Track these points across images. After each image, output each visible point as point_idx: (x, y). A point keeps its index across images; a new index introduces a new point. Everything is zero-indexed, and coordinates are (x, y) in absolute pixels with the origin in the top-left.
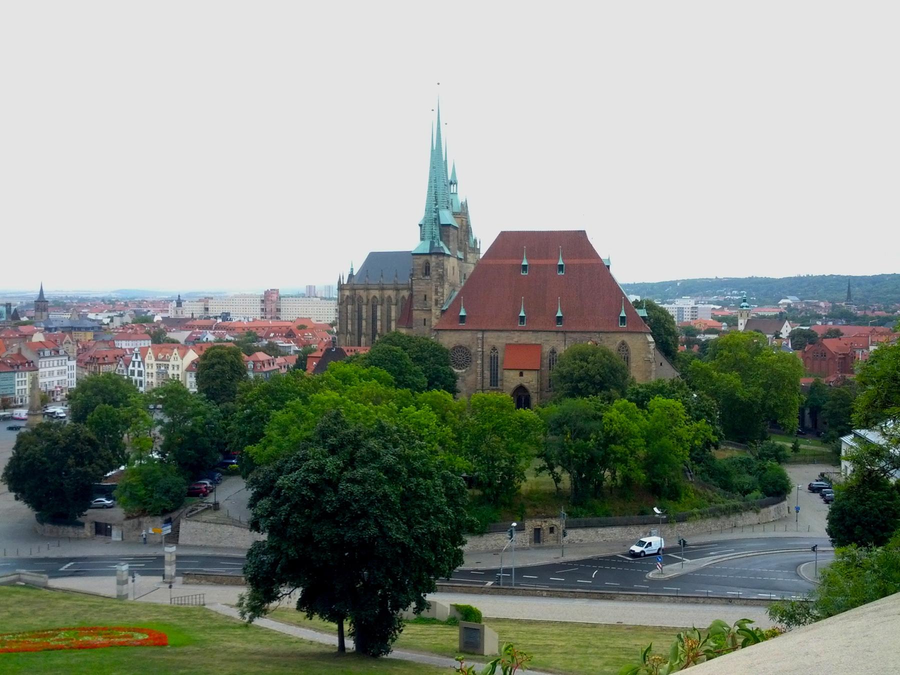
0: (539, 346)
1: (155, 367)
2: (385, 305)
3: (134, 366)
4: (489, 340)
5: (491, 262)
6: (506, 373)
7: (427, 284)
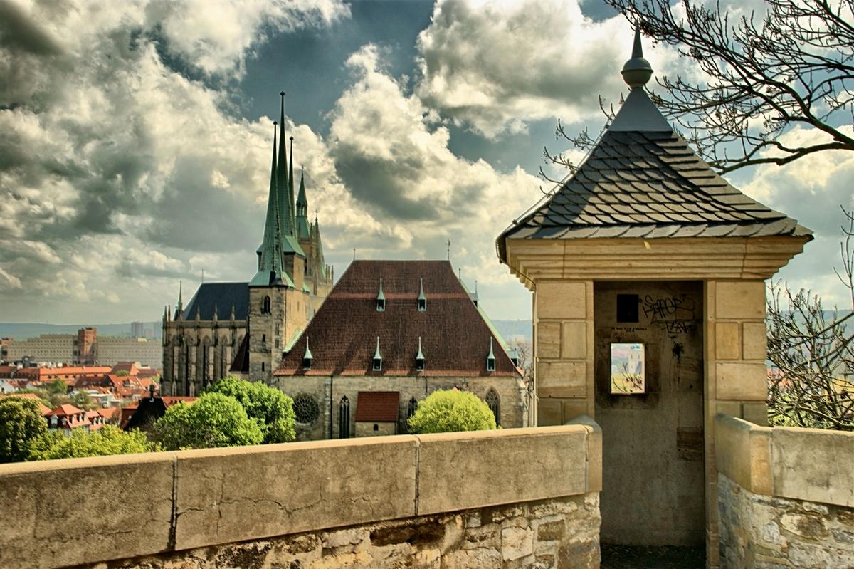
0: (396, 395)
2: (219, 347)
4: (338, 387)
5: (344, 295)
7: (266, 321)
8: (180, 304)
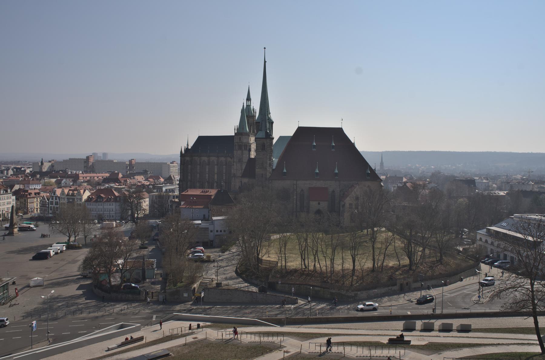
1: (66, 200)
3: (52, 199)
6: (311, 203)
8: (188, 145)
